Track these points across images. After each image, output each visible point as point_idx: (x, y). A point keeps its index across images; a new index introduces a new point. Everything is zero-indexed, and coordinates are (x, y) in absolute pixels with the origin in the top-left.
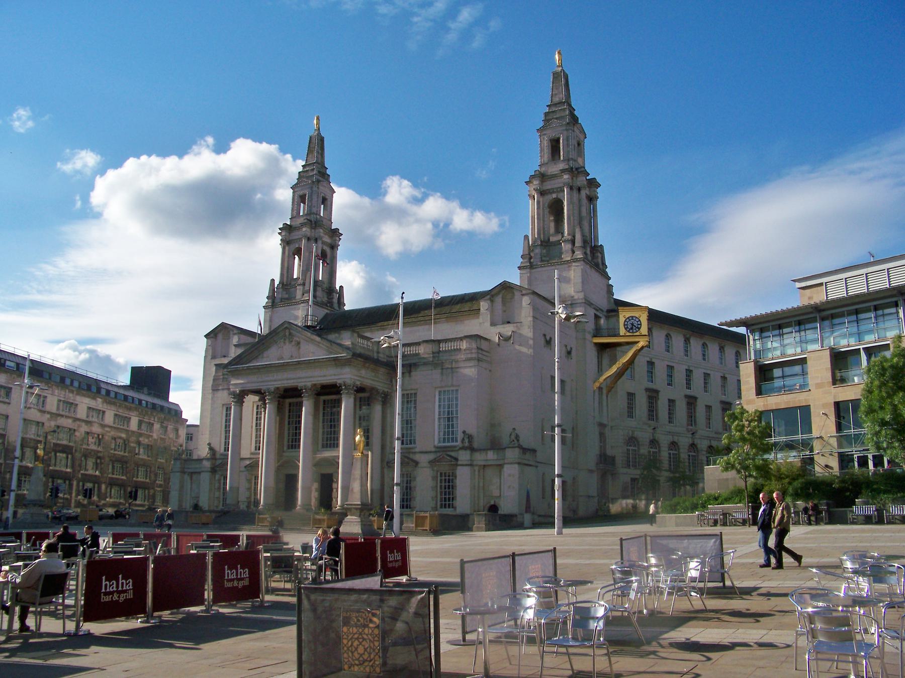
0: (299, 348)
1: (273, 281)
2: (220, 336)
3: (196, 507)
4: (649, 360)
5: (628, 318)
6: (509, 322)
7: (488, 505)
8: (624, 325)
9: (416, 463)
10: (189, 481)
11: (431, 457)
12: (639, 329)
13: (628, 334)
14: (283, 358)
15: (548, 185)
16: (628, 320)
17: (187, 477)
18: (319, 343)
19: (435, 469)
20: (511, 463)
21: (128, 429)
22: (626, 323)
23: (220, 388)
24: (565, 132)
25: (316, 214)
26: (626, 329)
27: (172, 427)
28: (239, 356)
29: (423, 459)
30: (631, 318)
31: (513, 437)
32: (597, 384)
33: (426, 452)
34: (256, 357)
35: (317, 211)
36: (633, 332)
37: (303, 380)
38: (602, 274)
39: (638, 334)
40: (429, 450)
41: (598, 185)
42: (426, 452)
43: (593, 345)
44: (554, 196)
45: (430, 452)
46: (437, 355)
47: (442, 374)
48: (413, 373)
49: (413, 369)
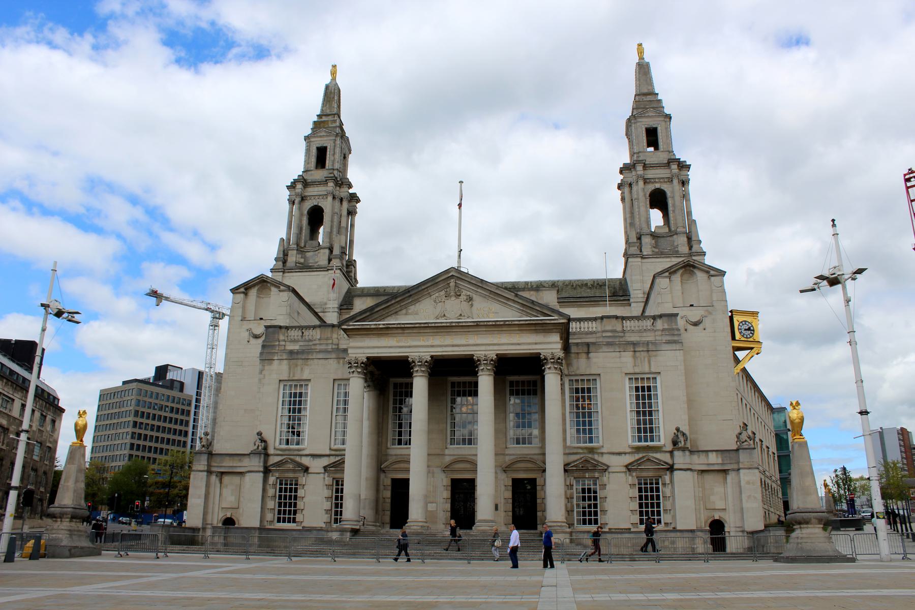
0: (472, 305)
1: (282, 240)
2: (253, 292)
3: (229, 522)
5: (741, 322)
6: (692, 305)
7: (710, 520)
8: (739, 329)
9: (605, 469)
10: (218, 485)
11: (628, 459)
12: (753, 334)
14: (444, 315)
15: (650, 174)
16: (741, 324)
17: (213, 478)
18: (508, 299)
19: (634, 474)
20: (750, 468)
21: (9, 414)
23: (276, 358)
24: (664, 123)
25: (340, 172)
27: (51, 417)
28: (371, 309)
29: (617, 463)
31: (744, 437)
33: (619, 454)
34: (396, 312)
35: (340, 168)
36: (747, 338)
37: (483, 348)
39: (751, 339)
40: (622, 451)
42: (619, 454)
44: (657, 186)
45: (625, 453)
46: (622, 334)
47: (634, 357)
48: (591, 355)
49: (591, 349)
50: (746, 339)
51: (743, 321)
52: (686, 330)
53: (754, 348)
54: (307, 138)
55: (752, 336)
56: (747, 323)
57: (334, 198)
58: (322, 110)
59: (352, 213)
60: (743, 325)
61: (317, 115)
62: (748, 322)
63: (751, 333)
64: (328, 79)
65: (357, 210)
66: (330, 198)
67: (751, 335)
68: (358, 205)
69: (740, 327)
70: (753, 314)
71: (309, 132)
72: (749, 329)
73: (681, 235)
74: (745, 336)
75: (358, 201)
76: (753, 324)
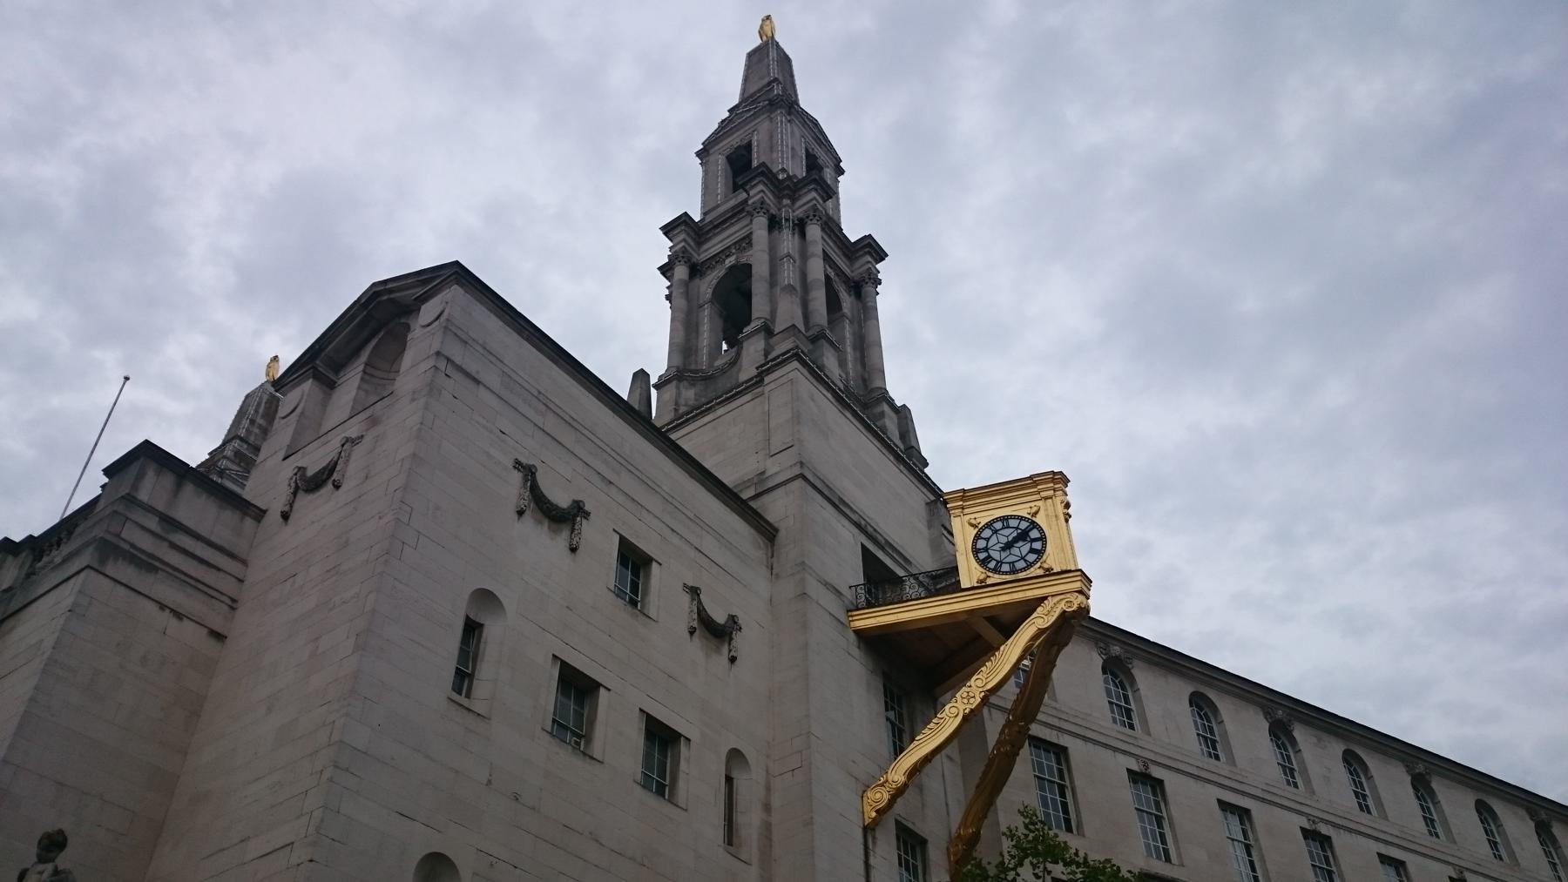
4: (1135, 767)
5: (989, 525)
8: (976, 551)
12: (1040, 553)
13: (996, 578)
15: (714, 246)
22: (981, 544)
26: (983, 563)
30: (998, 525)
32: (880, 796)
36: (1014, 571)
38: (898, 458)
41: (881, 255)
43: (852, 637)
44: (730, 261)
50: (1009, 578)
51: (997, 520)
52: (285, 516)
53: (1046, 598)
55: (1036, 561)
56: (1013, 523)
60: (996, 532)
62: (1014, 517)
63: (1032, 551)
67: (1031, 557)
69: (981, 544)
70: (1036, 484)
72: (1023, 536)
73: (755, 338)
74: (1006, 568)
76: (1039, 520)
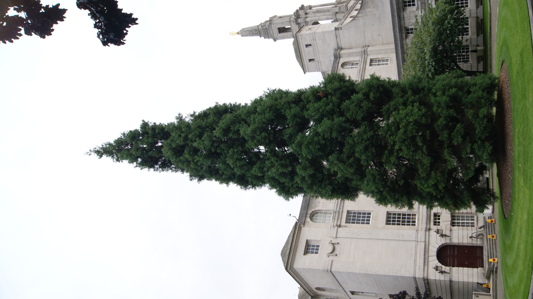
54: (275, 40)
57: (306, 18)
58: (258, 35)
59: (310, 7)
61: (261, 37)
64: (240, 36)
65: (308, 5)
66: (308, 19)
68: (305, 5)
71: (271, 40)
75: (303, 6)
